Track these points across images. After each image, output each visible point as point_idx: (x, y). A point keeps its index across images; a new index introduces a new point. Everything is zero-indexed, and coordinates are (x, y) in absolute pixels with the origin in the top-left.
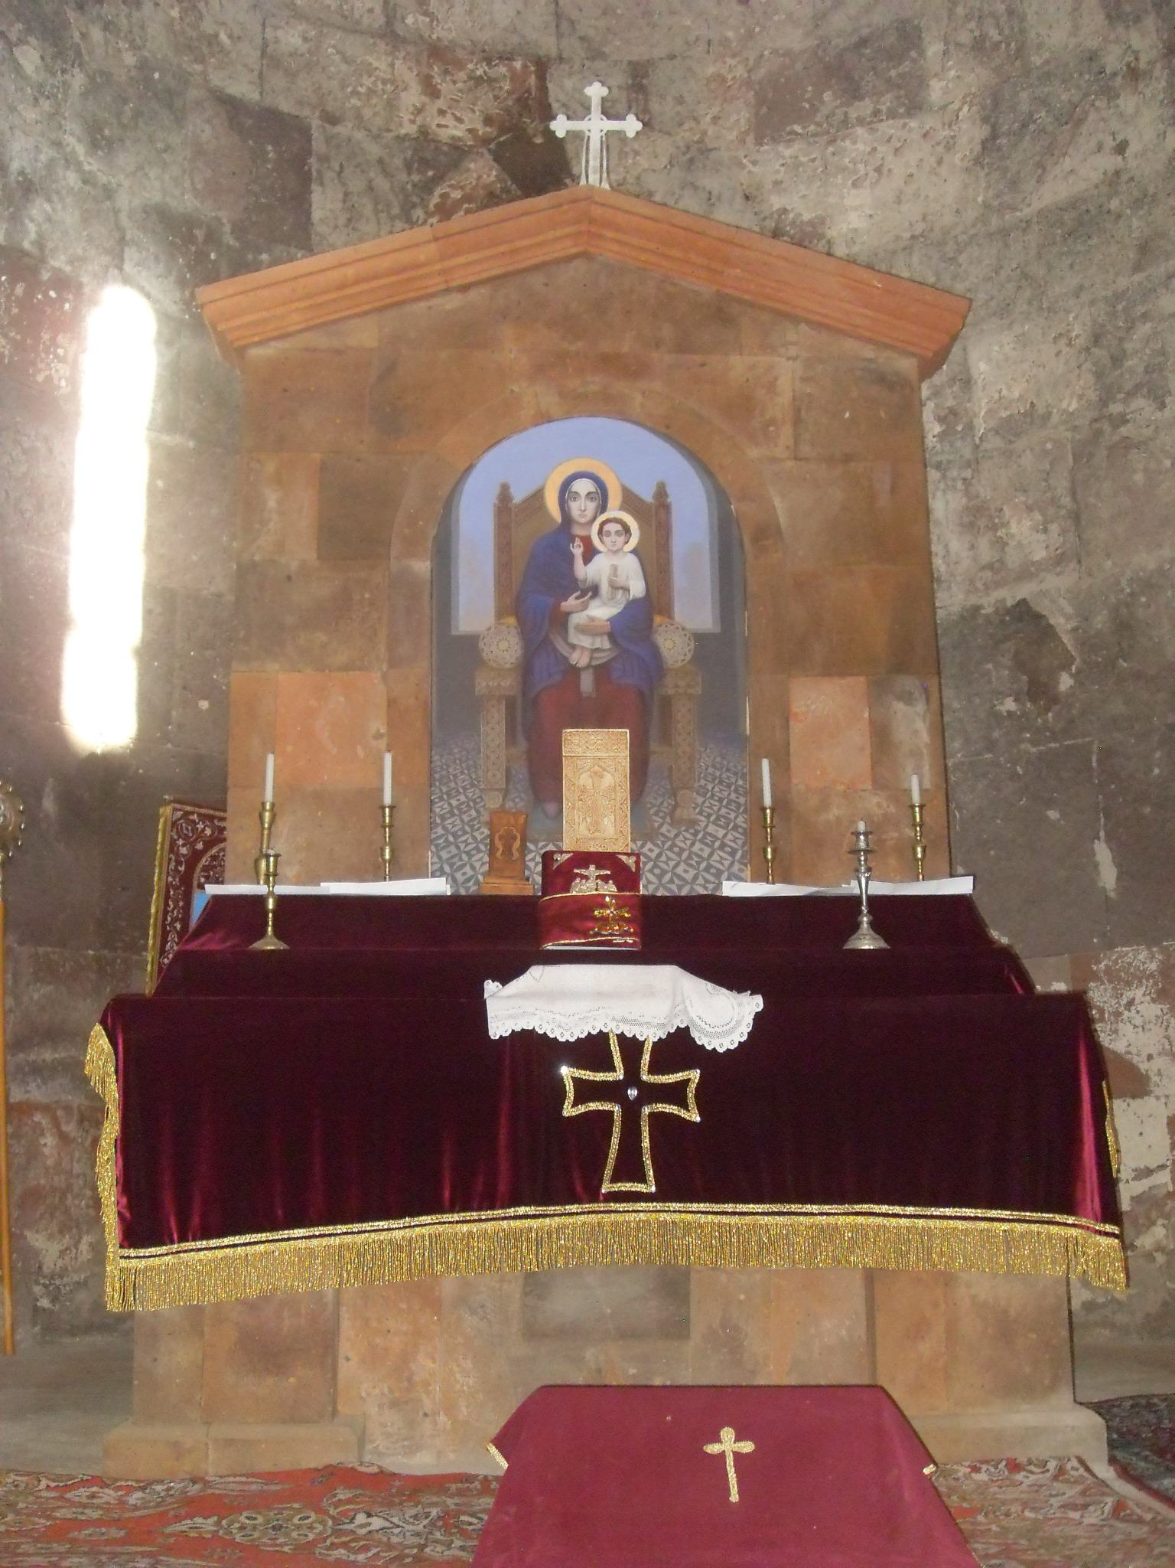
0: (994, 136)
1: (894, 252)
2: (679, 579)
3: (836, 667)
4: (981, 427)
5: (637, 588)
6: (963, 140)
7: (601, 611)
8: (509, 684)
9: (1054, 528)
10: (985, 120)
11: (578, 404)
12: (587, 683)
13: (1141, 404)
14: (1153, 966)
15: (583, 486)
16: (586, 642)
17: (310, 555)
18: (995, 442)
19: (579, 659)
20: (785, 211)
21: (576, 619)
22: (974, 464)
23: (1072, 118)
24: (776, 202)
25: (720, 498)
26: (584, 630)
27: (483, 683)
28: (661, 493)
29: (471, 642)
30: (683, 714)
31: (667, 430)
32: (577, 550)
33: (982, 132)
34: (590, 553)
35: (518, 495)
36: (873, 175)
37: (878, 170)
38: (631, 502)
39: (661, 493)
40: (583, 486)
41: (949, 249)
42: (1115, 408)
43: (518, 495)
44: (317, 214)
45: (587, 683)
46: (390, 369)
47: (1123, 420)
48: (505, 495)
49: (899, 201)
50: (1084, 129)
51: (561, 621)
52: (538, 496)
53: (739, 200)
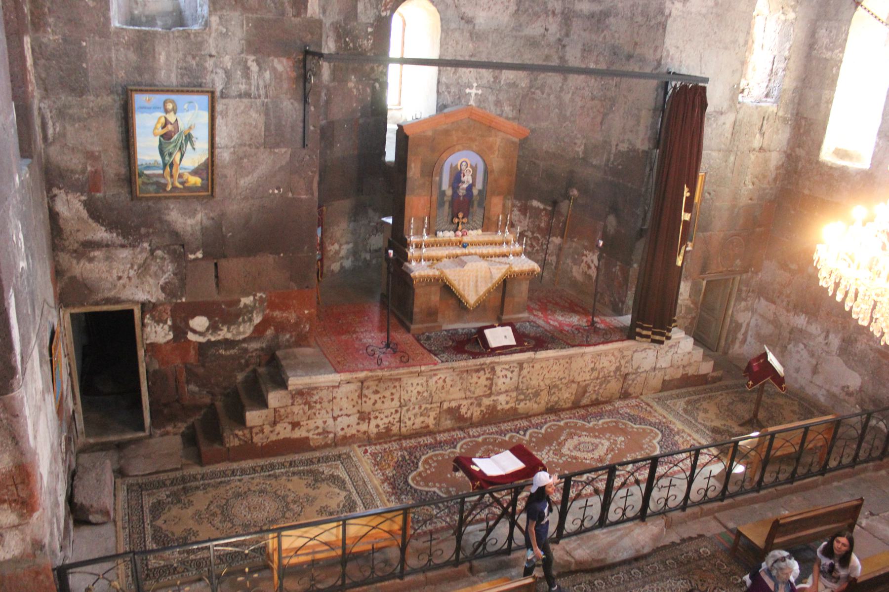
0: (518, 10)
1: (489, 32)
2: (477, 180)
3: (499, 195)
4: (502, 83)
5: (471, 182)
6: (510, 8)
7: (465, 186)
8: (450, 199)
9: (514, 112)
10: (517, 4)
11: (464, 148)
12: (461, 198)
13: (538, 92)
14: (519, 205)
15: (464, 164)
16: (462, 191)
17: (419, 175)
18: (505, 87)
19: (461, 194)
20: (464, 13)
21: (461, 187)
22: (499, 91)
23: (537, 15)
24: (463, 10)
25: (486, 165)
26: (463, 189)
27: (446, 199)
28: (476, 165)
29: (444, 191)
30: (476, 204)
31: (480, 154)
32: (462, 175)
33: (515, 8)
34: (464, 176)
35: (454, 165)
36: (487, 9)
37: (489, 8)
38: (471, 167)
39: (476, 165)
40: (464, 164)
41: (503, 36)
42: (533, 90)
43: (454, 165)
44: (359, 11)
45: (461, 198)
46: (434, 139)
47: (534, 93)
48: (452, 165)
49: (493, 18)
50: (540, 19)
51: (458, 187)
52: (457, 165)
53: (454, 7)
